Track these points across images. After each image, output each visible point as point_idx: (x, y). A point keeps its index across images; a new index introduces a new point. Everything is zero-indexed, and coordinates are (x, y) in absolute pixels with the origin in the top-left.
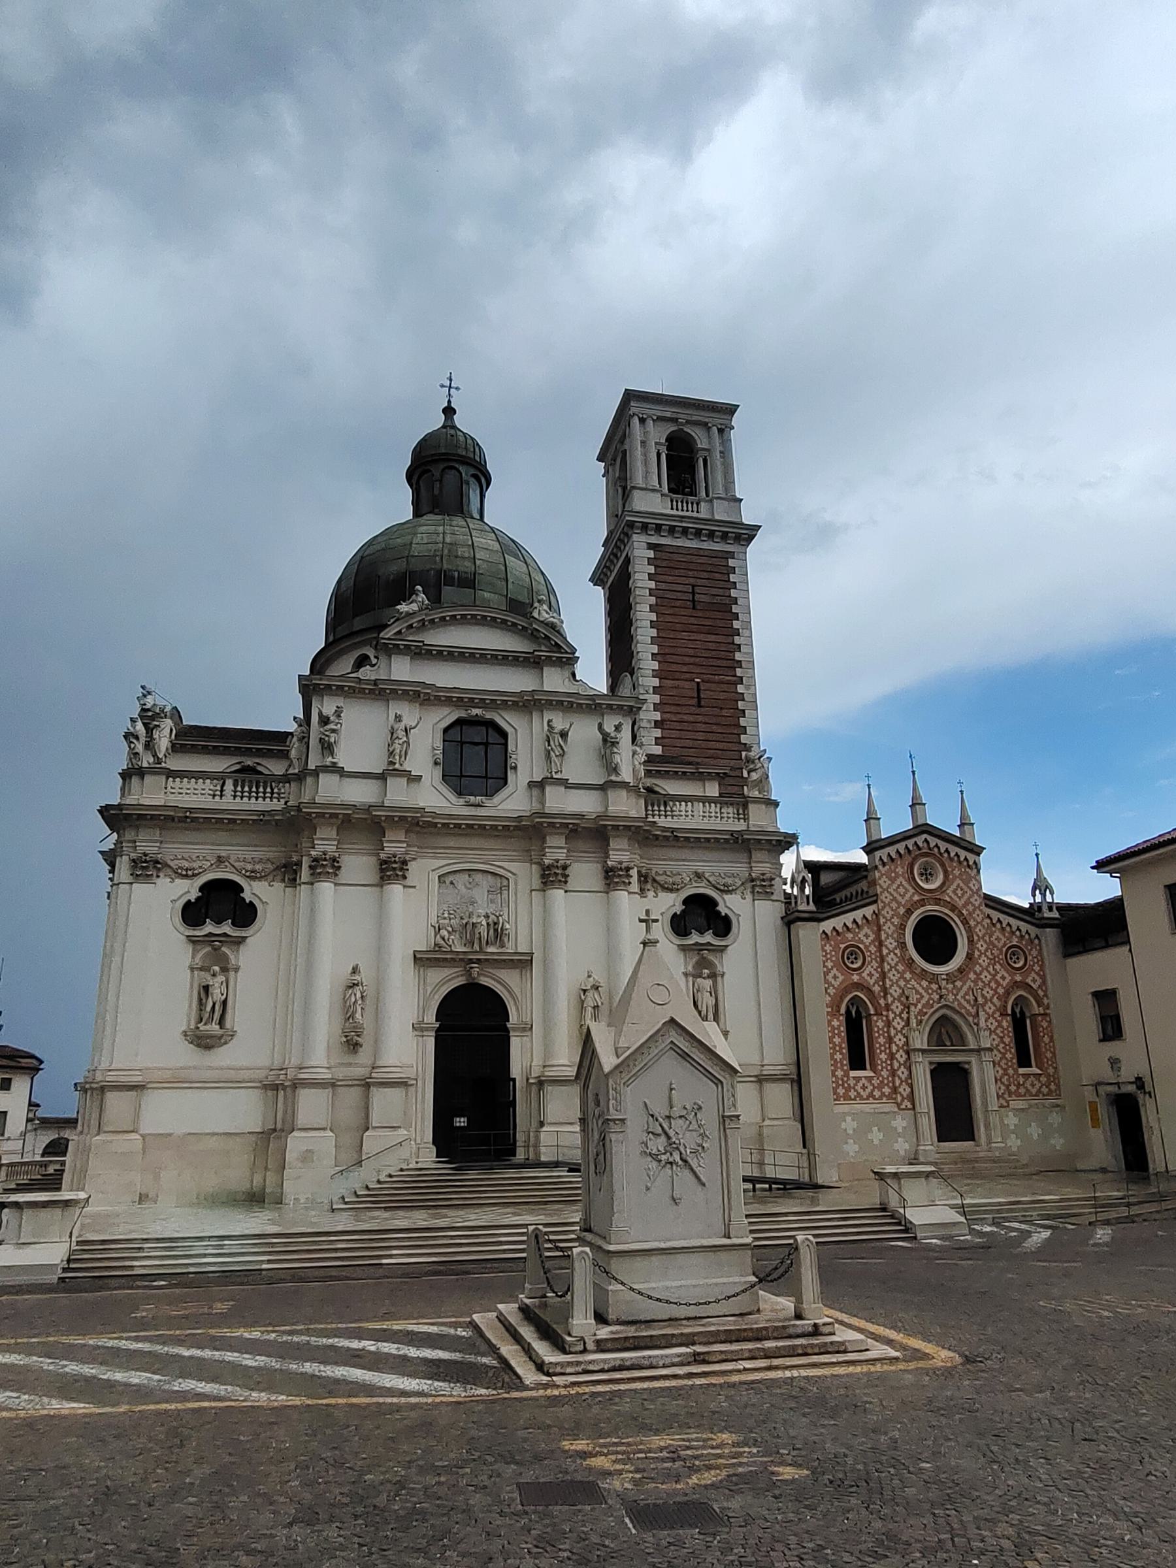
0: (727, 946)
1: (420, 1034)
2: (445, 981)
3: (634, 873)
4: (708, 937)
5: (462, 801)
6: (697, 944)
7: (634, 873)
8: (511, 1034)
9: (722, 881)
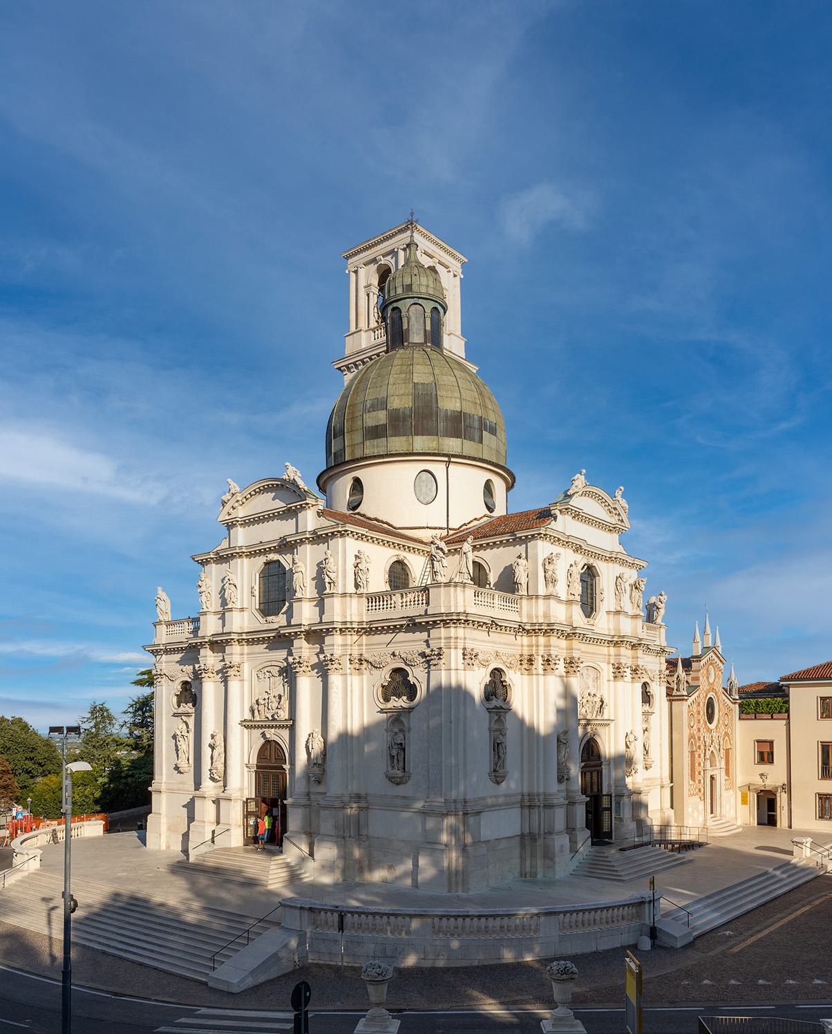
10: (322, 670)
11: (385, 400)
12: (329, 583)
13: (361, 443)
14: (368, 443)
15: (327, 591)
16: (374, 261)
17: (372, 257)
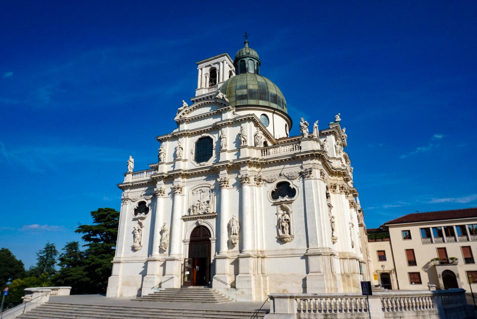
0: (293, 201)
1: (185, 243)
2: (192, 225)
3: (252, 179)
4: (286, 198)
5: (199, 164)
6: (281, 201)
7: (252, 179)
8: (212, 242)
9: (290, 175)
10: (240, 184)
11: (246, 85)
12: (243, 141)
13: (235, 101)
14: (238, 101)
15: (242, 145)
16: (210, 65)
17: (209, 64)
